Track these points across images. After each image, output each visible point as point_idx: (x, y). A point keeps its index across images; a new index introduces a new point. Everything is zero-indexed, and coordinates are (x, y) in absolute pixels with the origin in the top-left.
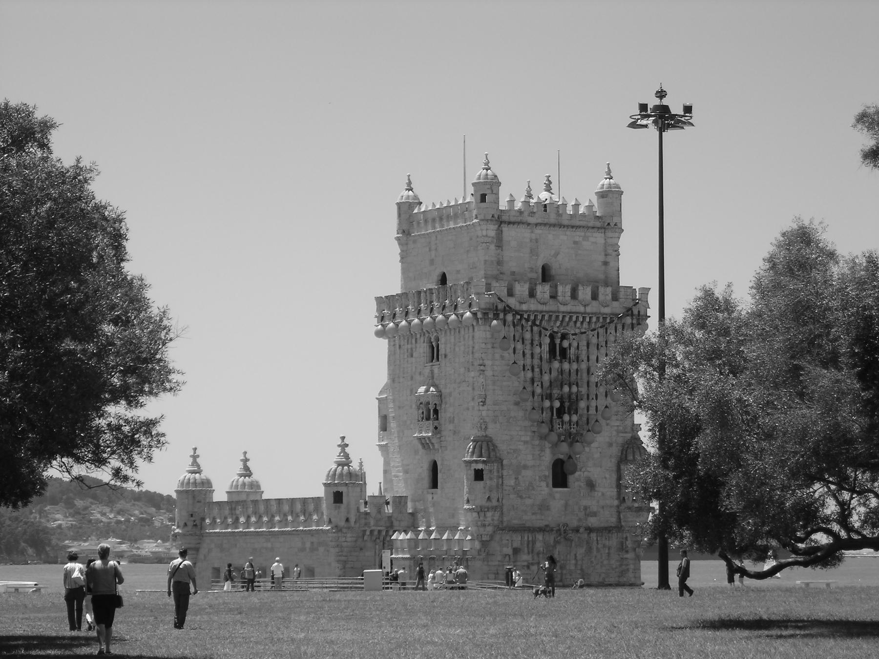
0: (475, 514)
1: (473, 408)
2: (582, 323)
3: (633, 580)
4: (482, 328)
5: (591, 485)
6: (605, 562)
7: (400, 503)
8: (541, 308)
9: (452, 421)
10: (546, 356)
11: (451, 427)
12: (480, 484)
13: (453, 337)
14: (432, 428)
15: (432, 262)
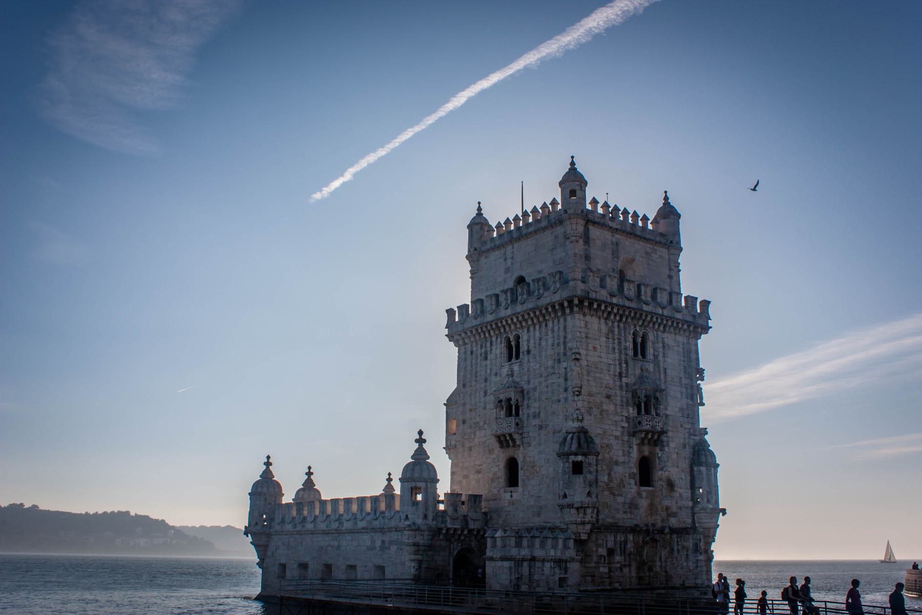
0: (573, 511)
1: (566, 399)
2: (659, 325)
3: (706, 583)
4: (577, 316)
5: (671, 485)
6: (685, 564)
7: (475, 502)
8: (627, 303)
9: (536, 416)
10: (631, 353)
11: (536, 422)
12: (579, 479)
13: (537, 334)
14: (513, 425)
15: (507, 270)
